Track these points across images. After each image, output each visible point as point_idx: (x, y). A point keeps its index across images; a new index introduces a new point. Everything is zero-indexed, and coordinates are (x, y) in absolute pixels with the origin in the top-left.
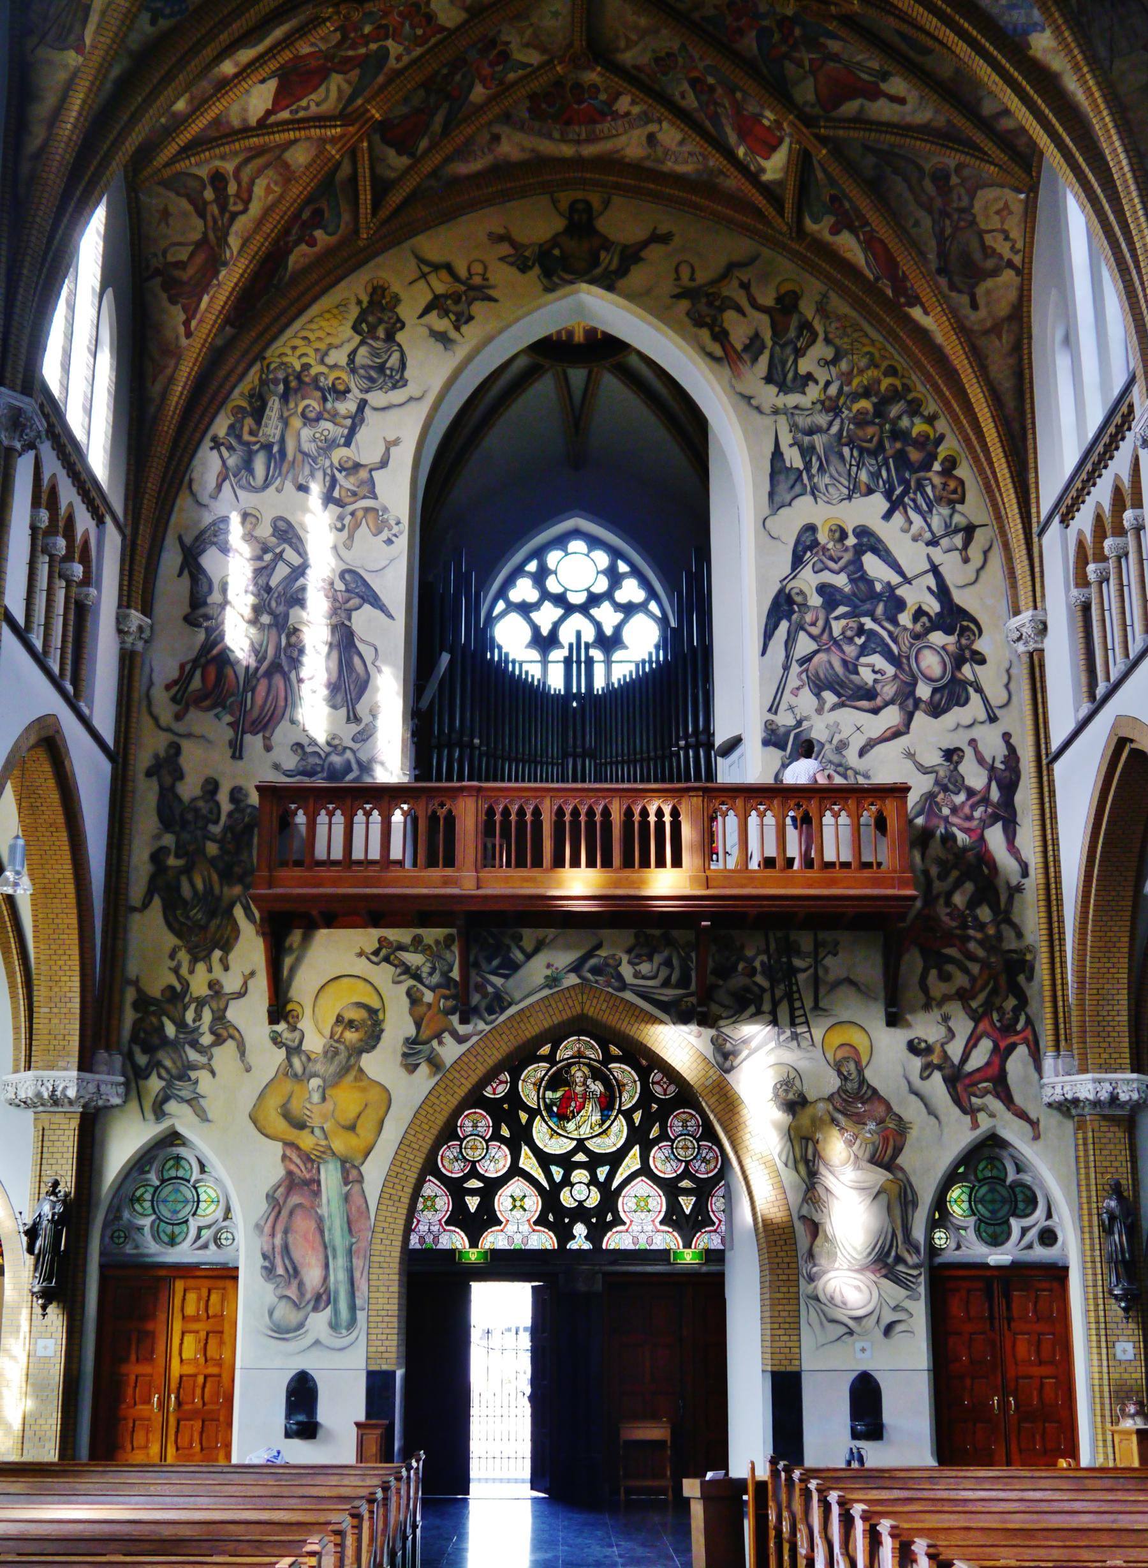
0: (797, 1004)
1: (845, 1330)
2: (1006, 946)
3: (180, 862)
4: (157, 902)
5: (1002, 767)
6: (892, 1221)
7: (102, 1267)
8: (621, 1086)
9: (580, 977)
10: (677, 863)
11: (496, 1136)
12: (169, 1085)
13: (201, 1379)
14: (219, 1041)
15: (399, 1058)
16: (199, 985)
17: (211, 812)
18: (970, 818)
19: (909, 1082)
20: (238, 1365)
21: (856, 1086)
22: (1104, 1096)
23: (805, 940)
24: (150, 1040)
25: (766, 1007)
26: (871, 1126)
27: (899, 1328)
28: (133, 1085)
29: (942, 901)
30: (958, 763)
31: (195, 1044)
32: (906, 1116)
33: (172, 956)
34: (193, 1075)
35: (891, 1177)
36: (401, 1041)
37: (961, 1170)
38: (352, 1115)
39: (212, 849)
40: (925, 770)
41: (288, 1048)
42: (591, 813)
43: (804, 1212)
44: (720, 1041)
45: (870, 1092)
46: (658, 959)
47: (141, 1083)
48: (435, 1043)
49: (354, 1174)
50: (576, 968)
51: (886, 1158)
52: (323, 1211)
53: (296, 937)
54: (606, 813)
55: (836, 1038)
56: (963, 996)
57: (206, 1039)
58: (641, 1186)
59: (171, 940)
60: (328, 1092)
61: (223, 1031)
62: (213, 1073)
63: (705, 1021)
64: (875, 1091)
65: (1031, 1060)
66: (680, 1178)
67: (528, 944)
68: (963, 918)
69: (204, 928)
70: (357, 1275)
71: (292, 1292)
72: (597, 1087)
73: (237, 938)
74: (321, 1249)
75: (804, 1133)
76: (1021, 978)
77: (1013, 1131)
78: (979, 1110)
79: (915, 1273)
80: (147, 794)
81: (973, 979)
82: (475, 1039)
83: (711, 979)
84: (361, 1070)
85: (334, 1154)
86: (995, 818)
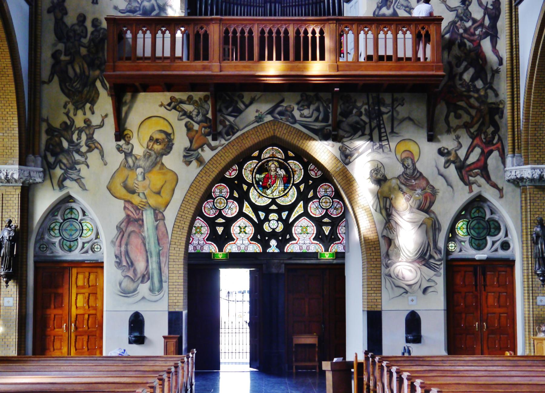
0: (383, 130)
1: (404, 291)
2: (490, 101)
3: (67, 58)
4: (56, 79)
5: (491, 7)
6: (428, 238)
7: (35, 262)
8: (294, 172)
9: (273, 117)
10: (322, 58)
11: (231, 197)
12: (66, 172)
13: (86, 316)
14: (90, 150)
15: (182, 158)
16: (79, 122)
17: (82, 32)
18: (474, 34)
19: (438, 170)
20: (105, 309)
21: (412, 171)
22: (536, 176)
23: (387, 98)
24: (55, 149)
25: (367, 132)
26: (419, 191)
27: (430, 290)
28: (48, 172)
29: (458, 77)
30: (469, 5)
31: (78, 152)
32: (436, 187)
33: (65, 107)
34: (78, 167)
35: (428, 216)
36: (183, 149)
37: (463, 213)
38: (158, 186)
39: (83, 51)
40: (451, 9)
41: (125, 153)
42: (278, 32)
43: (384, 234)
44: (344, 149)
45: (418, 174)
46: (312, 107)
47: (52, 171)
48: (200, 150)
49: (160, 216)
50: (271, 112)
51: (426, 207)
52: (145, 234)
53: (128, 97)
54: (286, 32)
55: (402, 147)
56: (467, 126)
57: (84, 149)
58: (304, 222)
59: (64, 99)
60: (146, 175)
61: (92, 145)
62: (88, 166)
63: (336, 139)
64: (421, 174)
65: (500, 158)
66: (323, 217)
67: (247, 100)
68: (468, 86)
69: (81, 92)
70: (163, 265)
71: (131, 274)
72: (282, 172)
73: (98, 97)
74: (144, 253)
75: (385, 195)
76: (497, 117)
77: (489, 194)
78: (473, 183)
79: (439, 263)
80: (48, 23)
81: (472, 118)
82: (220, 148)
83: (340, 118)
84: (162, 164)
85: (150, 206)
86: (486, 35)
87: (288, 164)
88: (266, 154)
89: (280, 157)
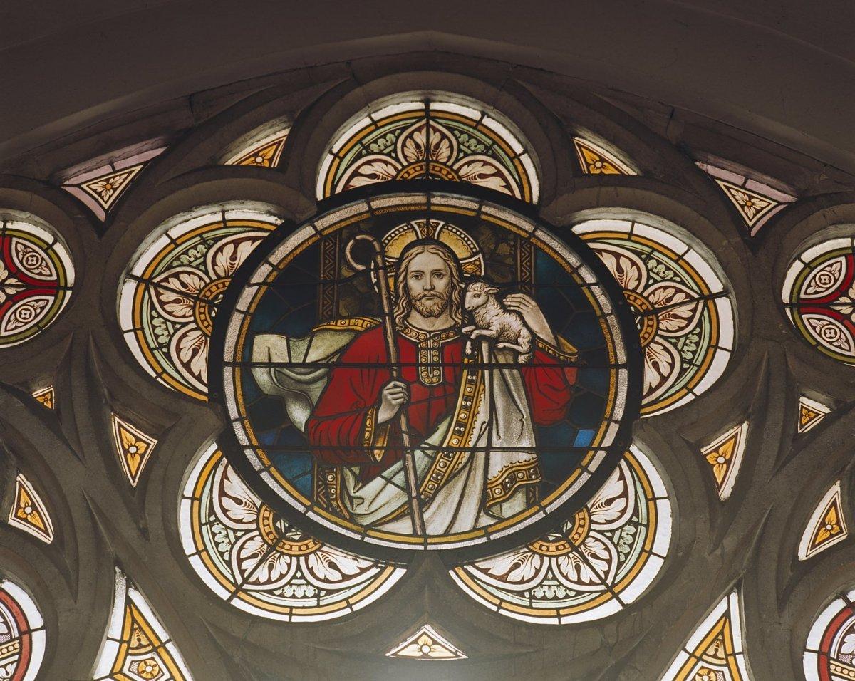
8: (635, 318)
72: (519, 321)
87: (578, 245)
88: (368, 142)
89: (494, 184)
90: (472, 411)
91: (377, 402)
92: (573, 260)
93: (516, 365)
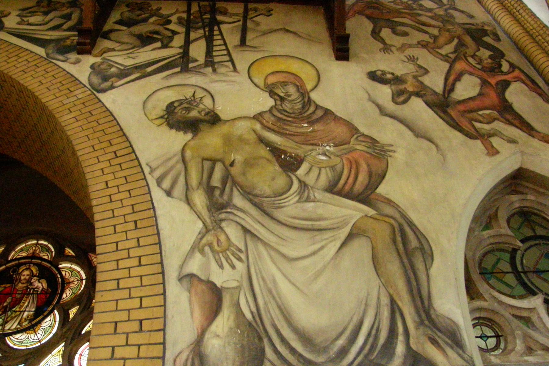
6: (386, 284)
19: (378, 106)
21: (299, 106)
43: (195, 266)
51: (359, 186)
72: (40, 285)
75: (209, 152)
78: (490, 135)
89: (46, 257)
90: (24, 303)
91: (5, 301)
92: (57, 272)
93: (37, 294)
